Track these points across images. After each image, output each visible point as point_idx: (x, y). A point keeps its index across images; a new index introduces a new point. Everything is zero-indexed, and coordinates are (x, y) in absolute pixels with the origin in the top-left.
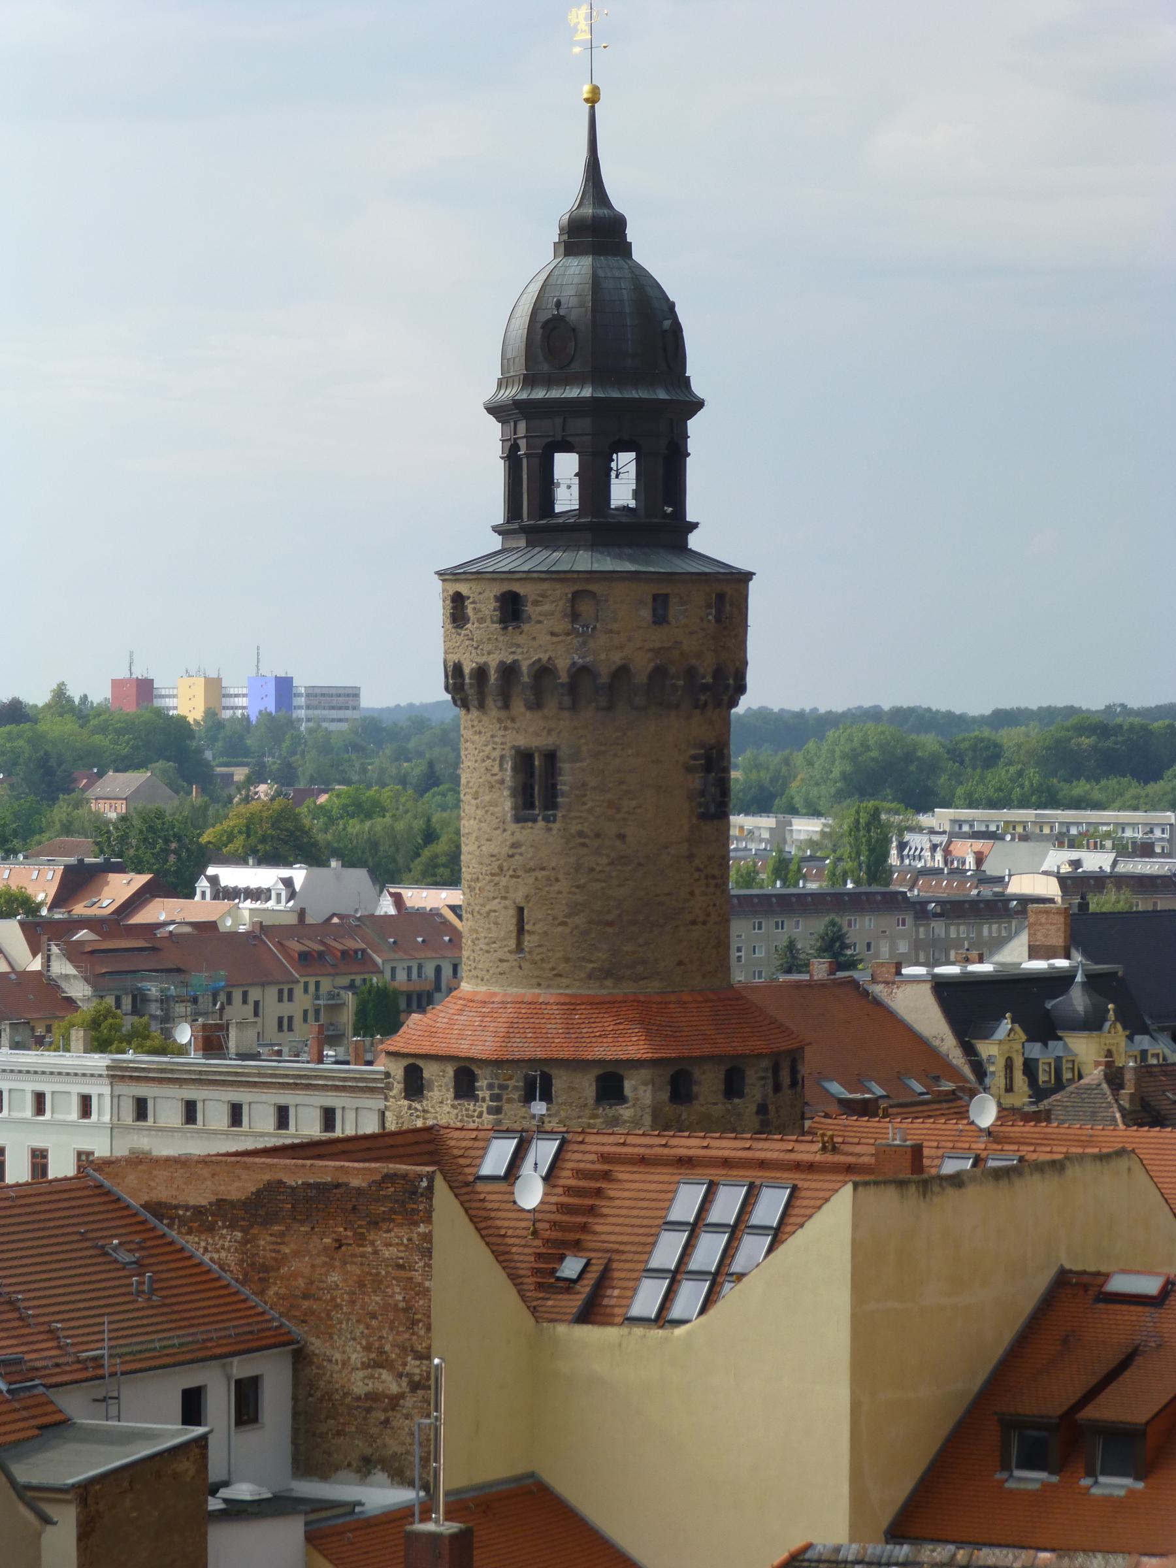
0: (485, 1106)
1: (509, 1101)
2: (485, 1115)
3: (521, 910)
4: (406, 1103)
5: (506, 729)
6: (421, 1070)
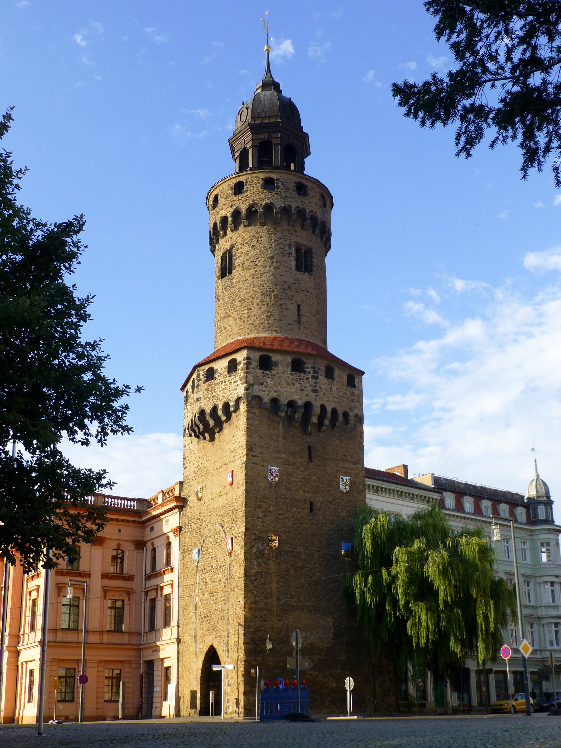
0: (310, 376)
1: (321, 375)
2: (310, 379)
3: (299, 306)
4: (261, 371)
5: (291, 234)
6: (270, 357)
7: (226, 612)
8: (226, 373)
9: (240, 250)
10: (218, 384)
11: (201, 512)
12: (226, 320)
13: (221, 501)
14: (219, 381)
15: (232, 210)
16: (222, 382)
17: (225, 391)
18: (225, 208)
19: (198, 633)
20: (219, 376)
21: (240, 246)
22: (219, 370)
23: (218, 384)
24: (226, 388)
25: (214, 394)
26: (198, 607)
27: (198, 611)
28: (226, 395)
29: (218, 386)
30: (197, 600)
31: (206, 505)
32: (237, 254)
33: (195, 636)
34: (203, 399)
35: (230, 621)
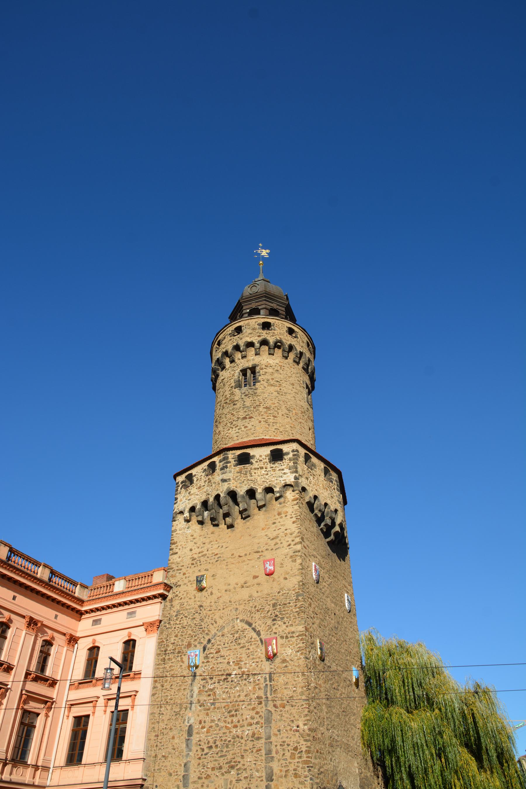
7: (263, 741)
8: (268, 461)
9: (264, 370)
10: (255, 469)
11: (204, 604)
12: (248, 420)
13: (245, 594)
14: (256, 466)
15: (260, 339)
16: (262, 468)
17: (267, 477)
18: (250, 336)
19: (191, 771)
20: (257, 462)
21: (264, 367)
22: (257, 456)
23: (255, 469)
24: (267, 474)
25: (249, 478)
26: (195, 731)
27: (195, 738)
28: (268, 481)
29: (256, 471)
30: (192, 721)
31: (214, 597)
32: (261, 372)
33: (185, 777)
34: (233, 481)
35: (274, 754)
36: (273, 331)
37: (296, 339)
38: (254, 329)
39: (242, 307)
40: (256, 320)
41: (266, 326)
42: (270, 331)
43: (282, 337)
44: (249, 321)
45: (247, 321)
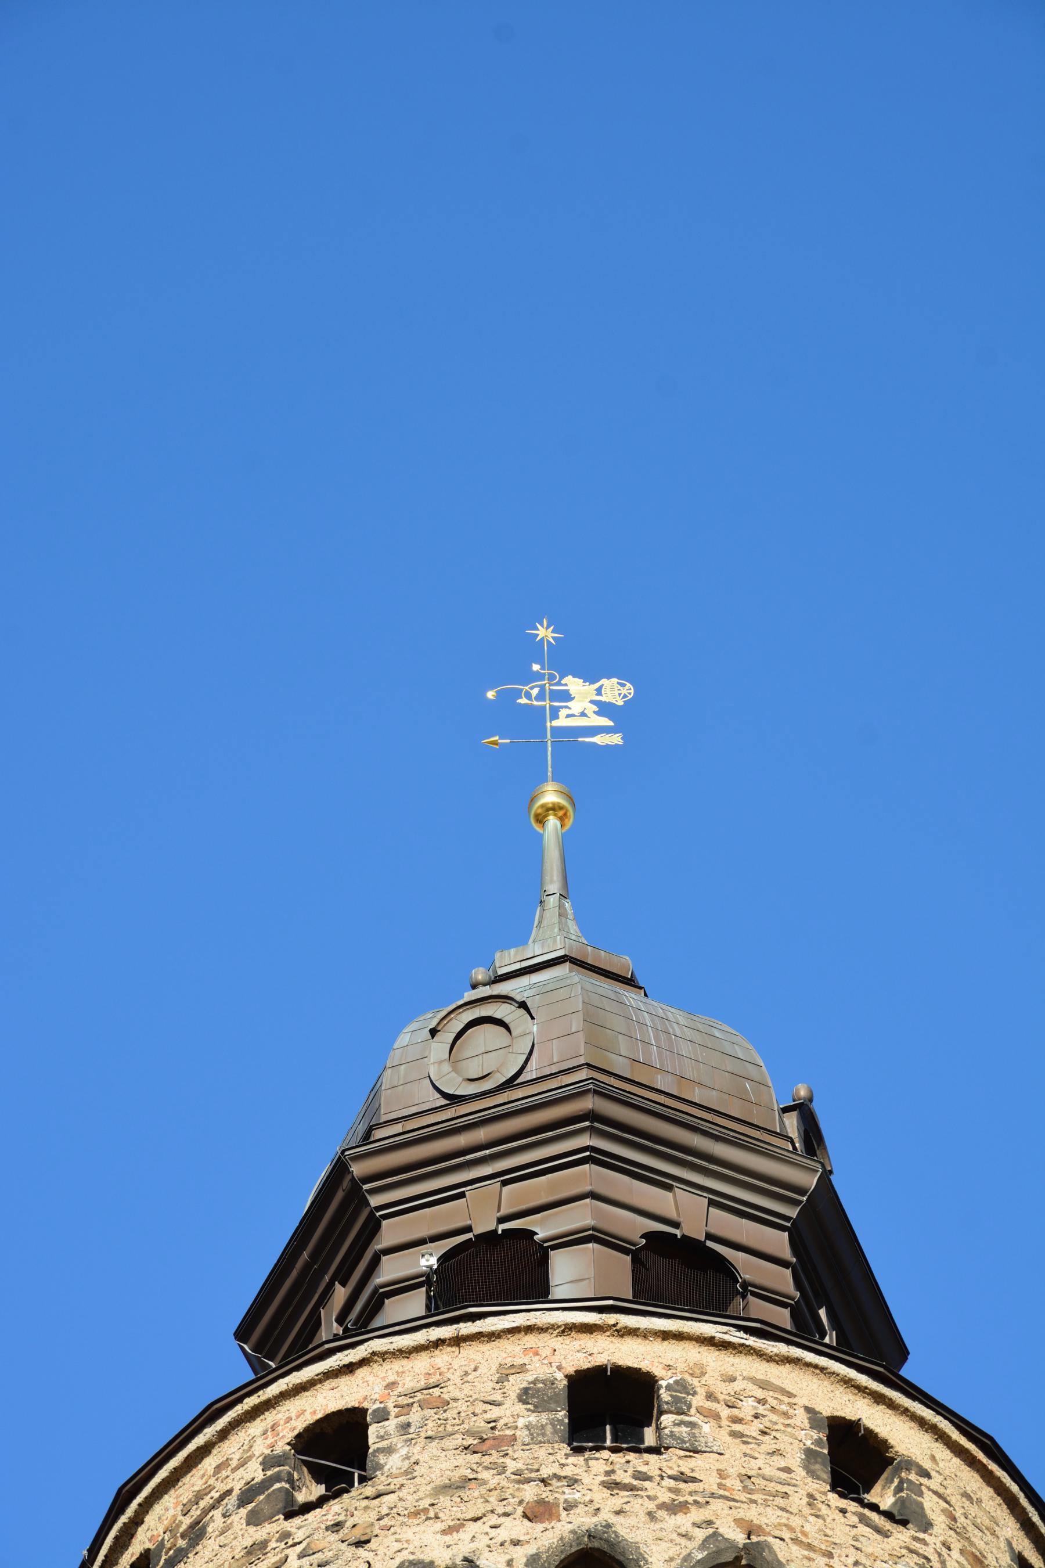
18: (450, 1508)
36: (673, 1461)
37: (902, 1536)
38: (486, 1442)
39: (373, 1227)
40: (508, 1351)
41: (609, 1409)
42: (652, 1464)
43: (767, 1517)
44: (442, 1358)
45: (422, 1363)
